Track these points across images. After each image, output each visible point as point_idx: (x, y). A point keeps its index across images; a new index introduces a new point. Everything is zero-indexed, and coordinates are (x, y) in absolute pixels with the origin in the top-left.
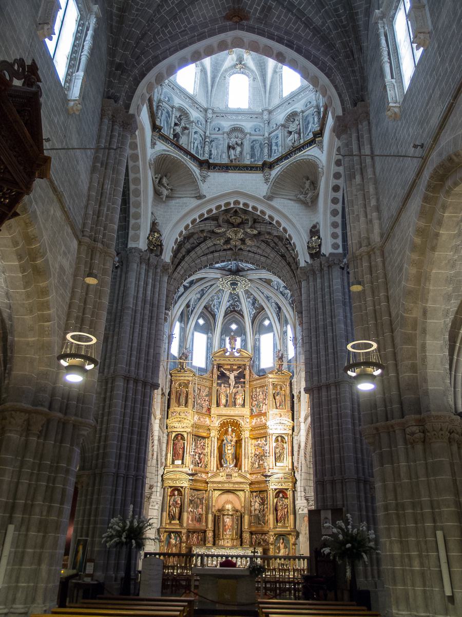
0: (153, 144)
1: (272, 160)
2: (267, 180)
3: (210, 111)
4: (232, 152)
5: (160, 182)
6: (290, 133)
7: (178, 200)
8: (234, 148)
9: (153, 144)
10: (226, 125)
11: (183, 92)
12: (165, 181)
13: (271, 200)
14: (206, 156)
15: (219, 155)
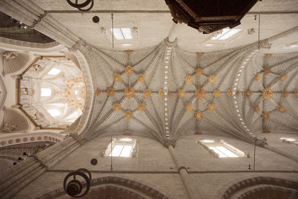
0: (35, 55)
1: (23, 108)
2: (13, 107)
3: (41, 80)
4: (25, 90)
5: (13, 55)
6: (36, 115)
7: (1, 63)
8: (26, 91)
9: (35, 55)
10: (35, 88)
11: (50, 70)
12: (14, 57)
13: (3, 110)
14: (24, 78)
15: (23, 83)
